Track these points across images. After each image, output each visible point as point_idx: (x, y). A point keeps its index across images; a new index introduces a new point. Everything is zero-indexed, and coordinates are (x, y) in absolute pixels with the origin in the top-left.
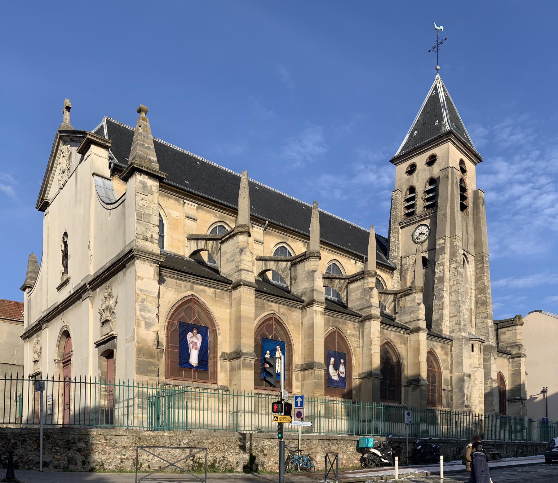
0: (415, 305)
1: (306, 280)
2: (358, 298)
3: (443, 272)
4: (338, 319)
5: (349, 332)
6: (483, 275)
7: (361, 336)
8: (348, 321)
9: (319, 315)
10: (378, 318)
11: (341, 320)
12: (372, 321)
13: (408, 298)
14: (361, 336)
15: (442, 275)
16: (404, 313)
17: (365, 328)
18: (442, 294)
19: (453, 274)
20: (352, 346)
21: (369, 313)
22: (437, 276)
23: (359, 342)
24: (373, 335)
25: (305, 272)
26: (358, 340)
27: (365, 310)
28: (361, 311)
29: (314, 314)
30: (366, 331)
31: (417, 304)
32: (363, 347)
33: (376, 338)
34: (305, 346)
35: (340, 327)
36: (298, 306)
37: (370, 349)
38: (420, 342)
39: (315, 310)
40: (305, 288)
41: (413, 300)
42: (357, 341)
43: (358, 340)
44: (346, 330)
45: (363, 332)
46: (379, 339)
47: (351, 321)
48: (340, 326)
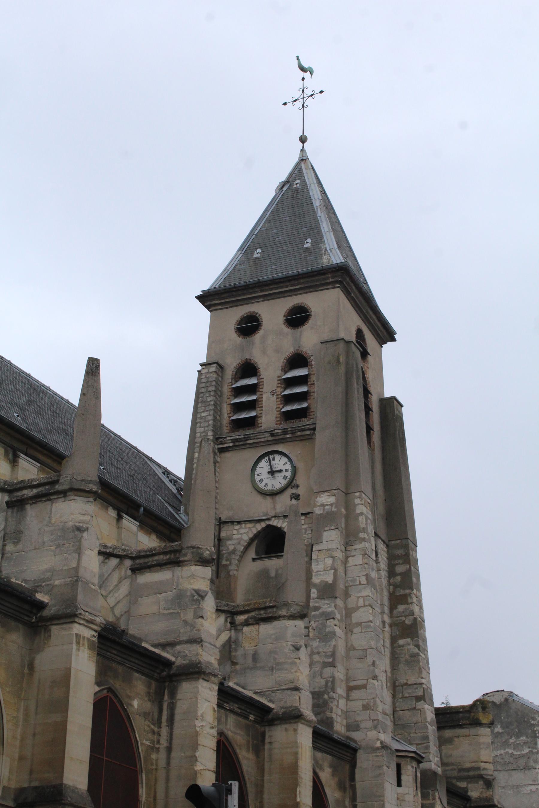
0: (287, 650)
1: (53, 548)
2: (159, 614)
3: (332, 572)
4: (114, 665)
5: (135, 703)
6: (407, 591)
7: (164, 718)
8: (136, 675)
9: (86, 649)
10: (215, 676)
11: (120, 669)
12: (201, 680)
13: (265, 629)
14: (164, 718)
15: (330, 580)
16: (254, 668)
17: (179, 696)
18: (330, 626)
19: (355, 580)
20: (142, 744)
21: (194, 659)
22: (316, 580)
23: (159, 734)
24: (202, 720)
25: (52, 528)
26: (156, 729)
27: (178, 648)
28: (169, 649)
29: (74, 646)
30: (181, 707)
31: (292, 648)
32: (169, 749)
33: (207, 730)
34: (34, 735)
35: (117, 686)
36: (26, 618)
37: (193, 759)
38: (300, 750)
39: (77, 635)
40: (52, 570)
41: (279, 637)
42: (153, 732)
43: (156, 729)
44: (129, 697)
45: (172, 708)
46: (214, 732)
47: (143, 674)
48: (117, 685)
